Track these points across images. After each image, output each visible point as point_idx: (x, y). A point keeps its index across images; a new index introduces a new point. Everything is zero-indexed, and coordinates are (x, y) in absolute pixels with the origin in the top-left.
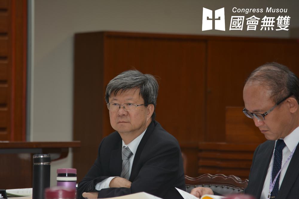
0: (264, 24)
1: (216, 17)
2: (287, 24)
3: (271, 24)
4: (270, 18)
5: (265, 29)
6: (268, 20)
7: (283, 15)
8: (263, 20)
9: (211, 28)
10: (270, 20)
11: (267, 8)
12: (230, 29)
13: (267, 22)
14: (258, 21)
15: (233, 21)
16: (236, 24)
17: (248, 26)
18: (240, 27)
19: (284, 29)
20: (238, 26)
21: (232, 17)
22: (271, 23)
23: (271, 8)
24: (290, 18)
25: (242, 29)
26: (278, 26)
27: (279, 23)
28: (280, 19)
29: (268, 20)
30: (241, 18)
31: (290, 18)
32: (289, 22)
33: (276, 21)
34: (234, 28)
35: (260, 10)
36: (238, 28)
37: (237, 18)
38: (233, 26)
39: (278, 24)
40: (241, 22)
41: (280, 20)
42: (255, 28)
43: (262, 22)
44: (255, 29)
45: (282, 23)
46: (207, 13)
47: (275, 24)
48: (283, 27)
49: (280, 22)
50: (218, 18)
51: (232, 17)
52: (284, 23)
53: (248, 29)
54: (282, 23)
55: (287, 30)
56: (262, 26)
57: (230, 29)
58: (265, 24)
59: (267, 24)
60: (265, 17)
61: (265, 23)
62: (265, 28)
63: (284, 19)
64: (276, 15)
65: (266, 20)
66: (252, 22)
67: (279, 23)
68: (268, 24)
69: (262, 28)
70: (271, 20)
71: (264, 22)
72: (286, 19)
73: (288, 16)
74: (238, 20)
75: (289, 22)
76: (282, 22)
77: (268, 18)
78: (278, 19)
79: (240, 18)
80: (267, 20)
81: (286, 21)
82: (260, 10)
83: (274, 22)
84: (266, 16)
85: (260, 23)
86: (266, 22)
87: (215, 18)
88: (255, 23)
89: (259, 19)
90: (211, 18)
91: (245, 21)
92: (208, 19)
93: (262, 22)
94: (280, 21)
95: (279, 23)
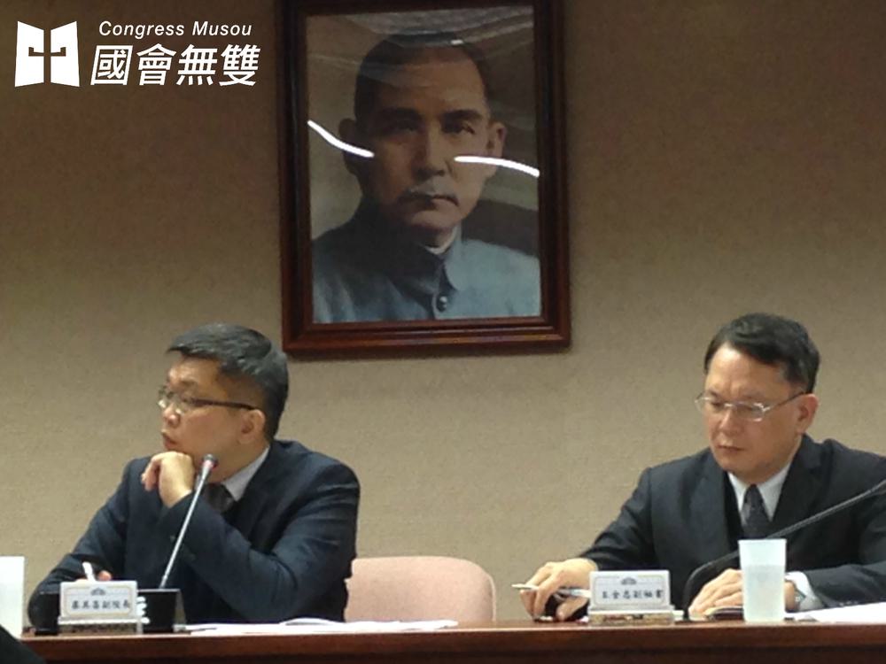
0: (187, 66)
1: (55, 48)
2: (250, 67)
3: (205, 68)
4: (203, 51)
5: (191, 82)
6: (199, 57)
7: (241, 41)
8: (185, 58)
9: (40, 79)
10: (203, 56)
11: (196, 23)
12: (94, 82)
13: (195, 61)
14: (169, 60)
15: (100, 59)
16: (109, 67)
17: (143, 73)
18: (119, 76)
19: (242, 81)
20: (116, 73)
21: (99, 48)
22: (206, 65)
23: (206, 23)
24: (259, 50)
25: (124, 82)
26: (225, 73)
27: (229, 65)
28: (231, 53)
29: (199, 57)
30: (123, 52)
31: (259, 50)
32: (256, 62)
33: (221, 60)
34: (105, 78)
35: (175, 30)
36: (115, 78)
37: (112, 52)
38: (100, 74)
39: (226, 67)
40: (122, 62)
41: (231, 56)
42: (163, 78)
43: (181, 61)
44: (162, 83)
45: (236, 65)
46: (28, 36)
47: (218, 67)
48: (239, 77)
49: (230, 62)
50: (59, 51)
53: (142, 82)
54: (236, 65)
55: (252, 83)
56: (180, 72)
57: (94, 82)
58: (190, 68)
60: (191, 49)
61: (191, 65)
62: (191, 79)
64: (220, 43)
65: (192, 57)
66: (155, 63)
67: (230, 67)
68: (198, 68)
69: (182, 78)
70: (207, 57)
71: (187, 62)
72: (249, 53)
73: (255, 46)
74: (116, 56)
75: (256, 62)
76: (237, 62)
77: (197, 51)
78: (226, 54)
79: (120, 50)
80: (196, 56)
81: (248, 59)
82: (175, 30)
83: (215, 61)
84: (191, 46)
85: (177, 66)
87: (53, 51)
88: (161, 66)
90: (42, 51)
91: (135, 60)
92: (32, 52)
93: (181, 61)
94: (230, 59)
95: (229, 65)
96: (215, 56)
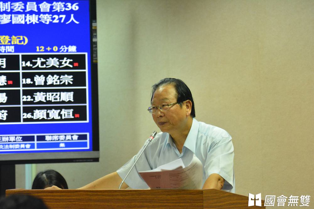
0: (290, 201)
2: (308, 201)
3: (295, 202)
4: (295, 197)
5: (291, 205)
6: (294, 199)
16: (269, 201)
17: (278, 203)
18: (272, 204)
19: (306, 205)
20: (271, 203)
24: (310, 197)
27: (302, 201)
28: (303, 197)
29: (294, 199)
38: (267, 203)
39: (301, 201)
40: (273, 200)
43: (289, 200)
44: (284, 206)
47: (299, 201)
51: (266, 196)
52: (306, 199)
55: (308, 206)
56: (289, 203)
59: (292, 201)
60: (291, 196)
63: (306, 197)
67: (302, 200)
69: (289, 204)
71: (290, 200)
74: (271, 198)
75: (309, 200)
77: (293, 197)
78: (301, 197)
81: (307, 199)
84: (292, 196)
85: (288, 201)
86: (292, 200)
88: (283, 201)
89: (287, 197)
91: (277, 199)
93: (289, 200)
95: (302, 201)
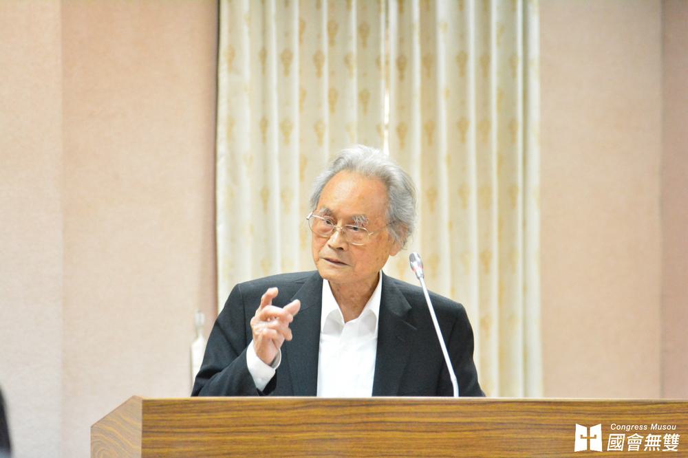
2: (676, 443)
4: (656, 436)
7: (672, 432)
9: (585, 448)
12: (608, 449)
13: (652, 441)
14: (641, 440)
19: (672, 449)
20: (618, 446)
21: (611, 435)
22: (656, 443)
23: (656, 425)
25: (622, 450)
37: (616, 437)
42: (638, 448)
44: (638, 450)
52: (672, 441)
55: (676, 450)
57: (608, 449)
58: (650, 443)
63: (673, 437)
64: (663, 433)
67: (667, 444)
69: (646, 448)
71: (648, 441)
74: (618, 438)
77: (653, 436)
78: (665, 438)
85: (644, 443)
89: (642, 437)
96: (660, 439)
